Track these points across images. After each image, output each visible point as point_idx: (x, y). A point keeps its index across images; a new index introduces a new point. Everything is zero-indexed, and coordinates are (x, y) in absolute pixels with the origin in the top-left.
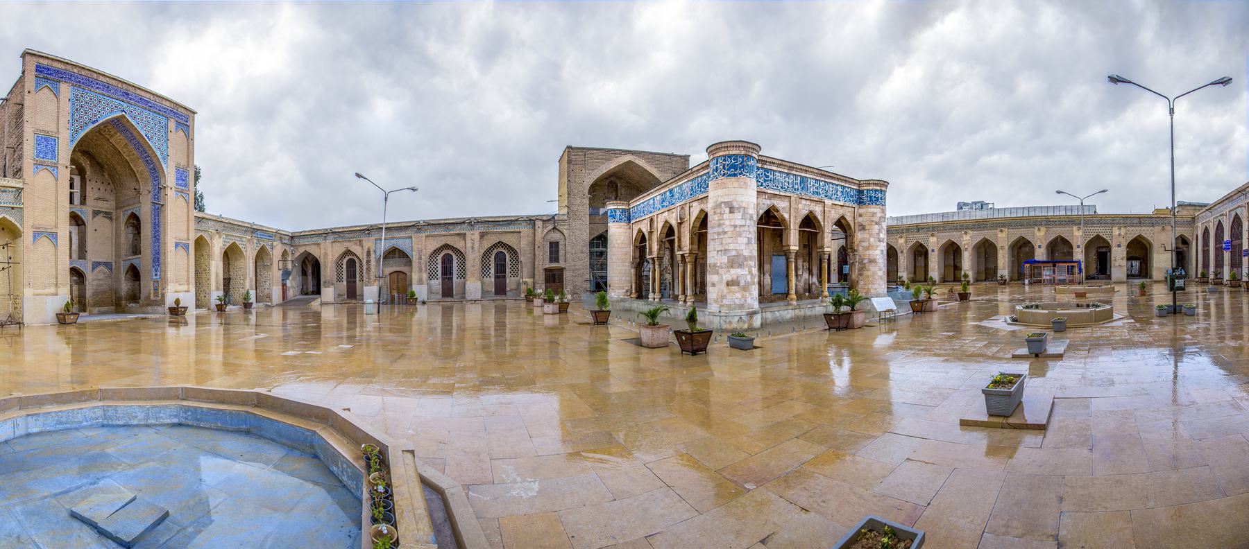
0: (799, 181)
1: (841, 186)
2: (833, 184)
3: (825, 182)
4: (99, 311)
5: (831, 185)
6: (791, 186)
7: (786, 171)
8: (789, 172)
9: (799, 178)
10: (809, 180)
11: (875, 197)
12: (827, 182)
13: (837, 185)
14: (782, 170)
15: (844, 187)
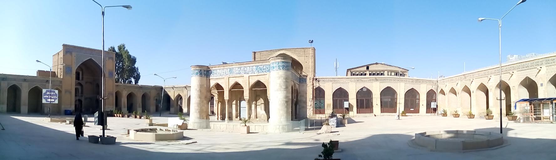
0: (229, 71)
1: (256, 66)
2: (249, 67)
3: (244, 67)
4: (77, 105)
5: (248, 68)
6: (224, 74)
7: (222, 68)
8: (224, 68)
9: (229, 69)
10: (234, 69)
11: (273, 67)
12: (246, 67)
13: (253, 66)
14: (220, 68)
15: (258, 66)
